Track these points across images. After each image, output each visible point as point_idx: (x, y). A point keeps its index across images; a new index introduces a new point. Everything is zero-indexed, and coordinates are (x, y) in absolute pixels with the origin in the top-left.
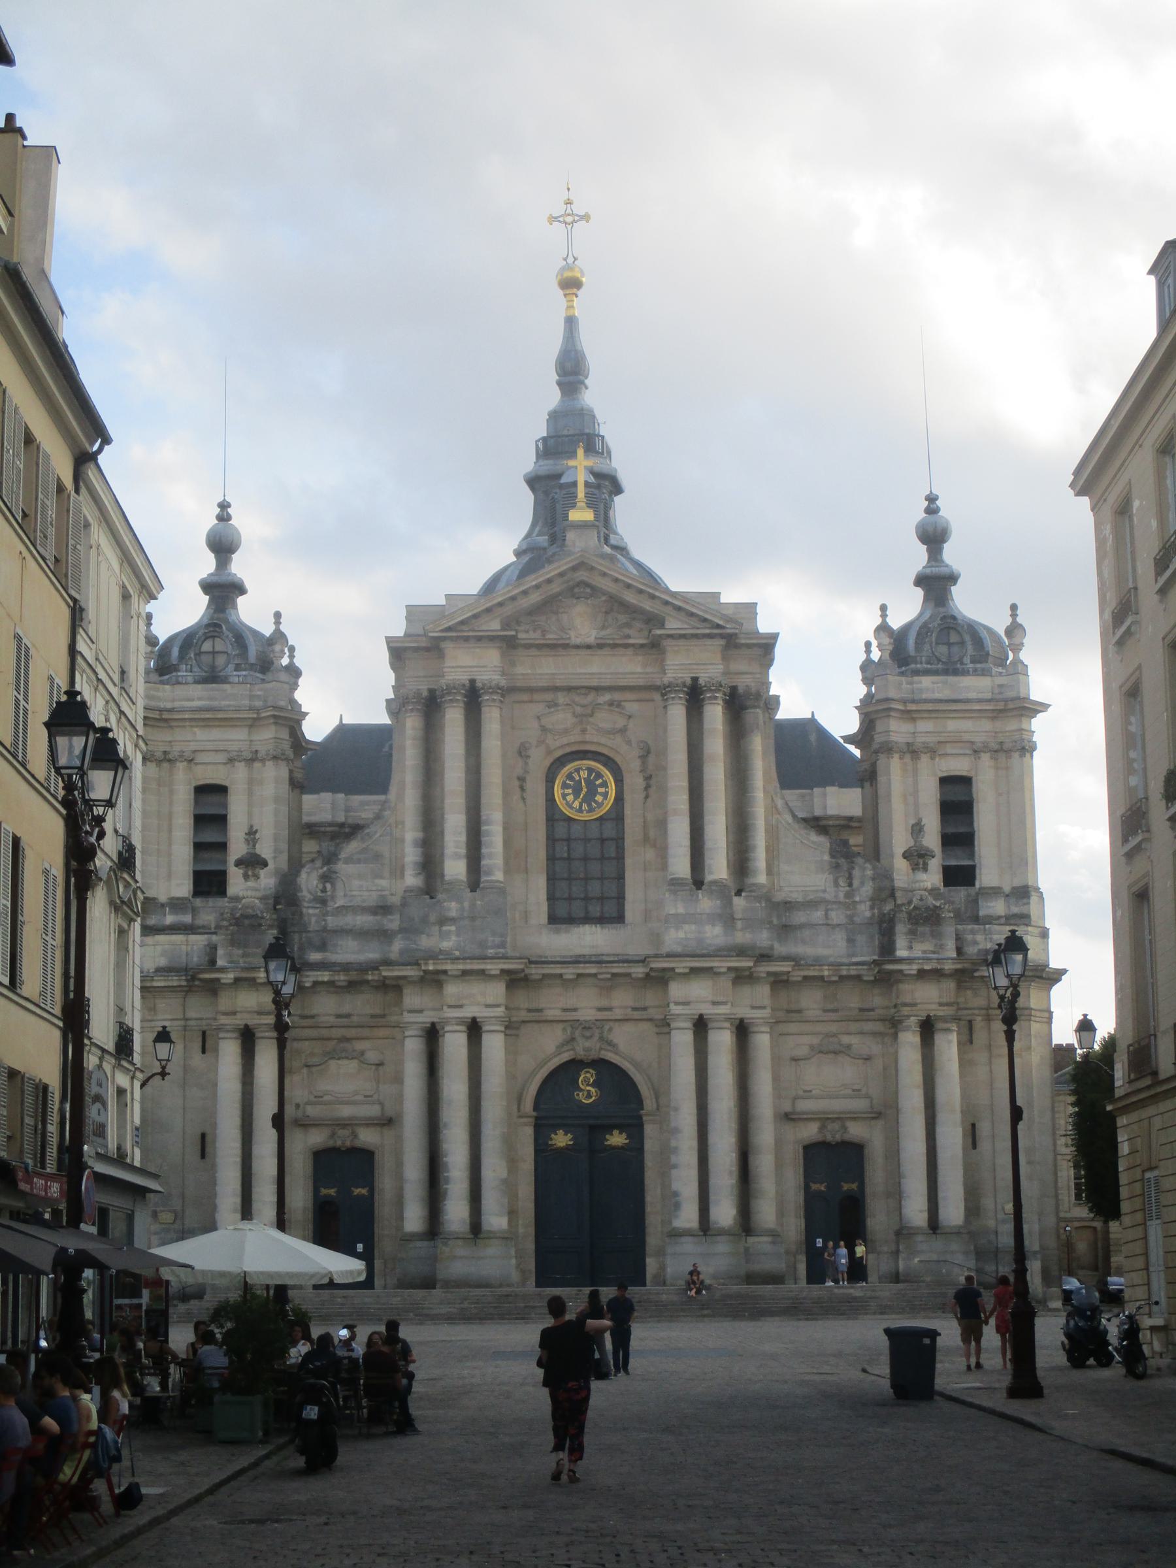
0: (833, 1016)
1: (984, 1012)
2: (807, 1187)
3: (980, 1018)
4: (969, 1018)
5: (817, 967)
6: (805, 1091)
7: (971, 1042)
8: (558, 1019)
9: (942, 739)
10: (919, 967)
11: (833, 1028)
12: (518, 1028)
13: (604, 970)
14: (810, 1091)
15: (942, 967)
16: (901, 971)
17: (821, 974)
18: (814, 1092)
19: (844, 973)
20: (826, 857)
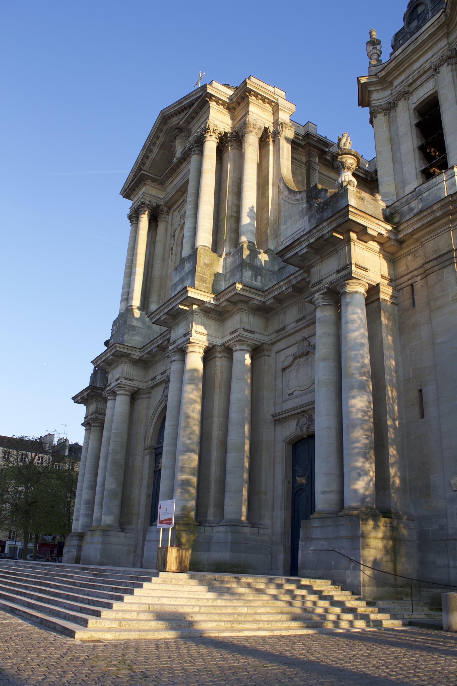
0: (302, 324)
1: (420, 271)
2: (294, 481)
3: (419, 278)
4: (410, 282)
5: (277, 286)
6: (290, 395)
7: (414, 305)
8: (161, 380)
9: (411, 81)
10: (307, 243)
11: (305, 333)
12: (149, 393)
13: (164, 339)
14: (292, 393)
15: (323, 233)
16: (297, 253)
17: (281, 290)
18: (295, 393)
19: (294, 282)
20: (305, 205)
